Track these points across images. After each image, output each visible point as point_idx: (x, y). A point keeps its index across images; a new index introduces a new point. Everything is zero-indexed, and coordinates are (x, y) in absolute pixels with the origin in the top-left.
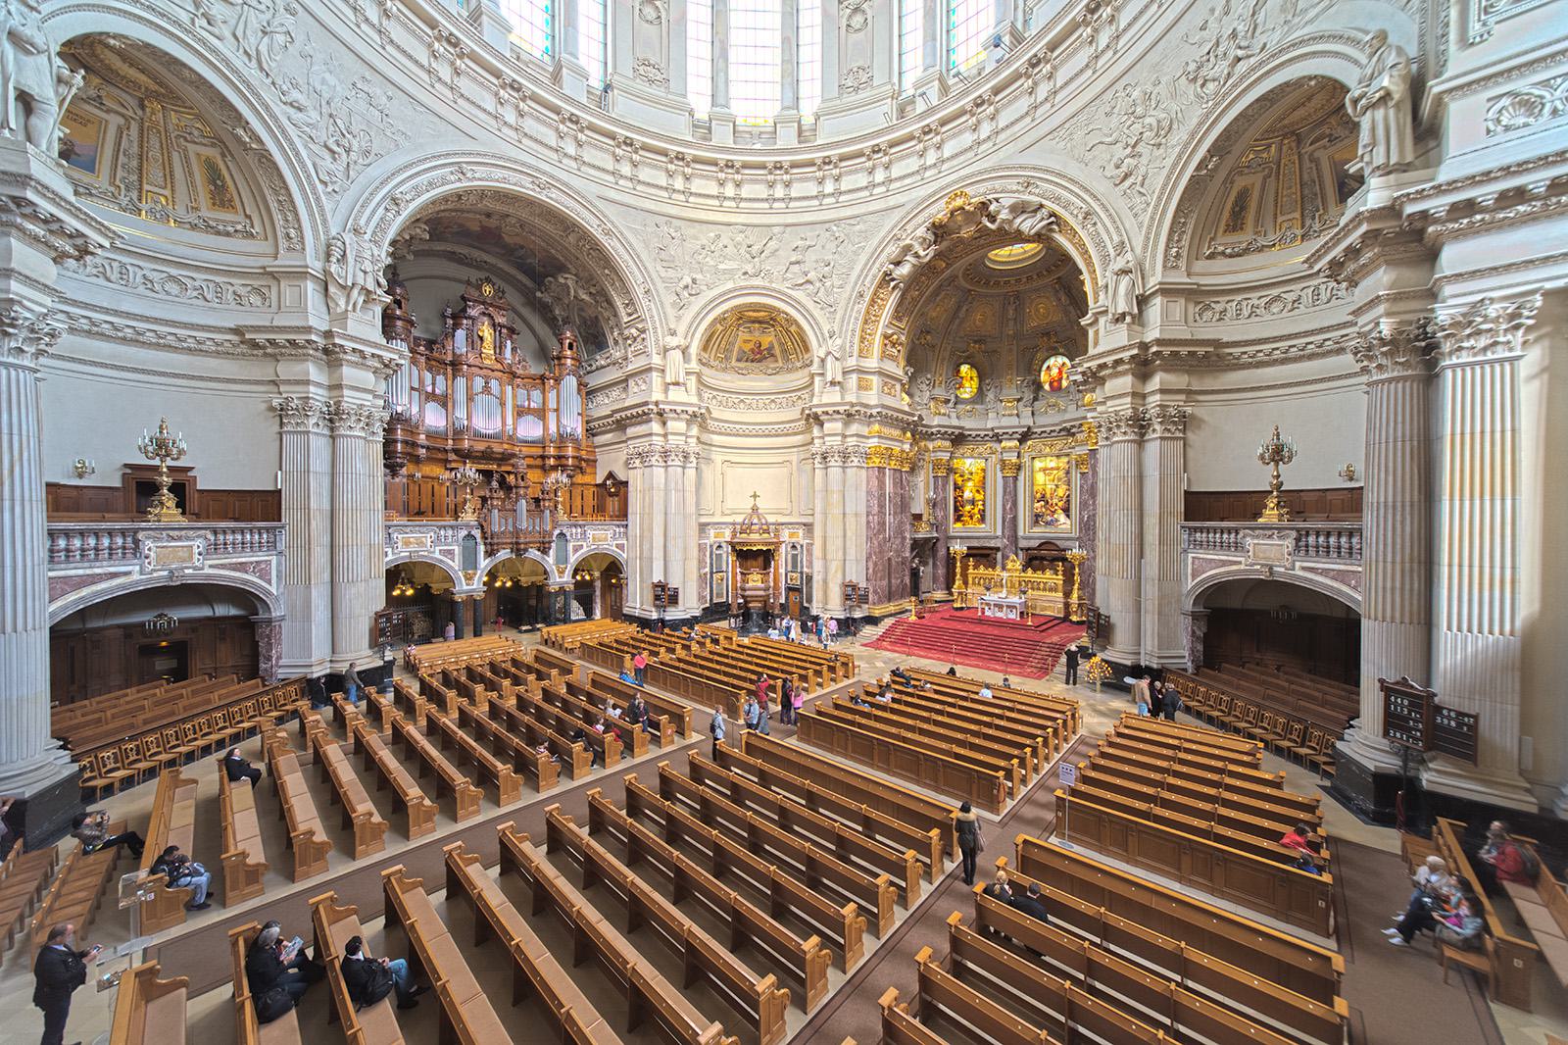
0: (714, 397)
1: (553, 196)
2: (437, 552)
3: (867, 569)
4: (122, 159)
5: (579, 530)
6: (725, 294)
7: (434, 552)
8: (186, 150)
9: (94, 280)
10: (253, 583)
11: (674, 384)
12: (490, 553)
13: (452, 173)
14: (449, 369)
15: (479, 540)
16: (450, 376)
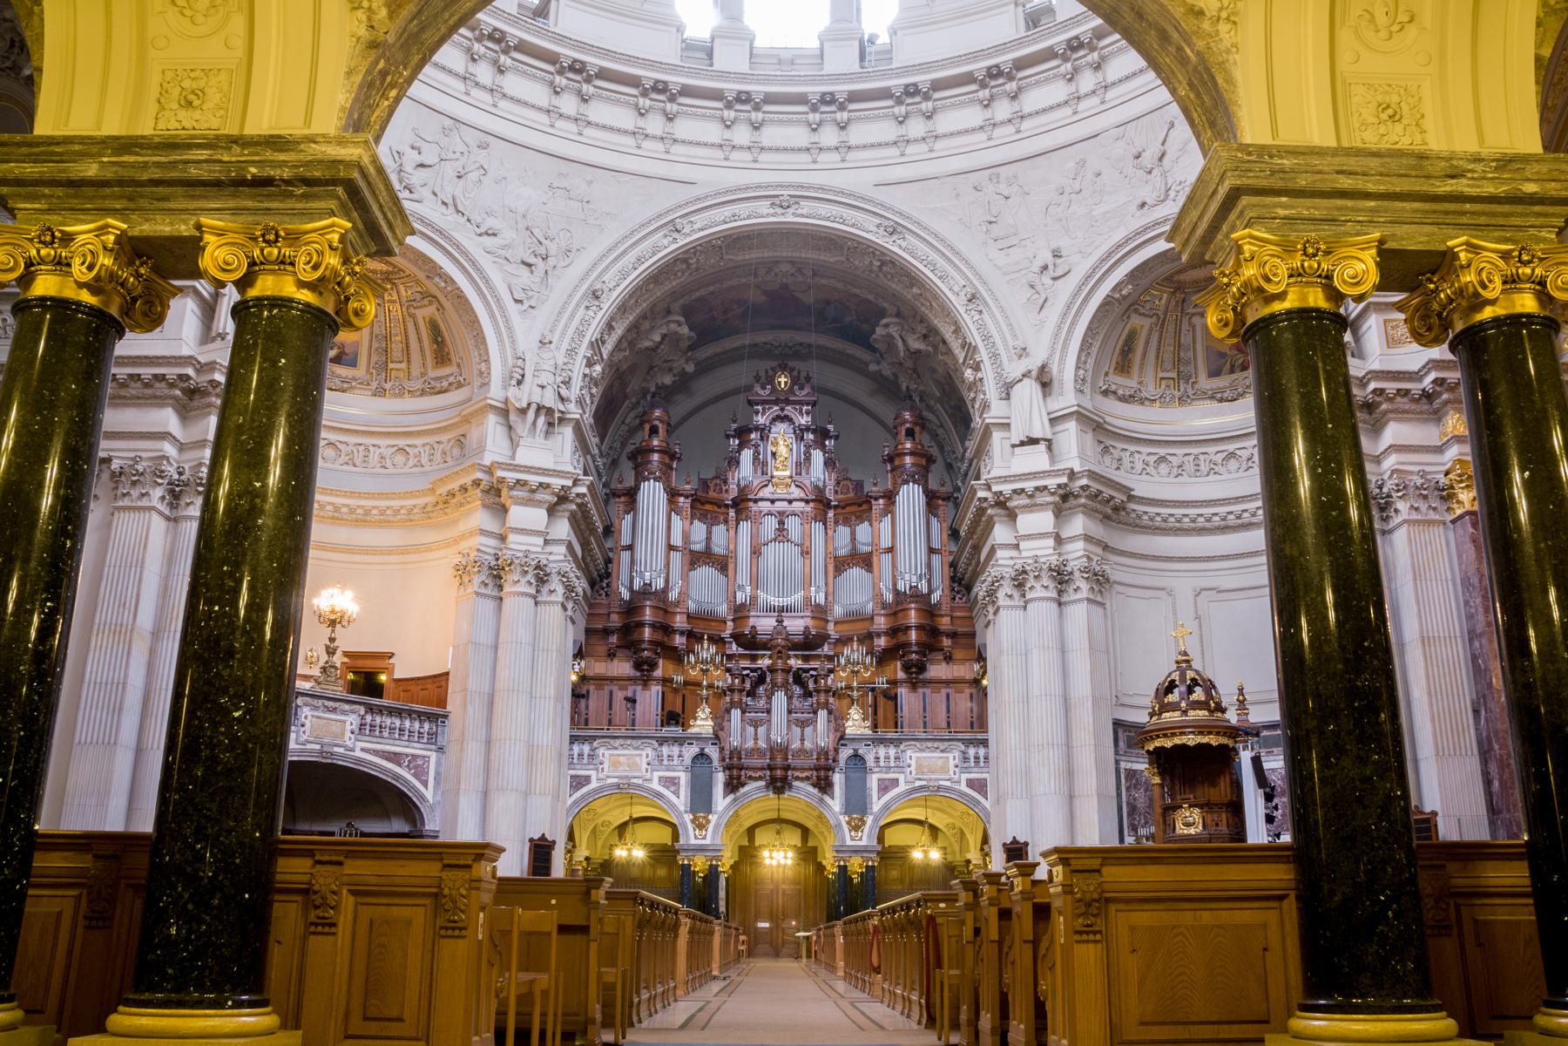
0: (1162, 459)
1: (804, 211)
2: (656, 780)
3: (1488, 783)
4: (375, 345)
5: (892, 751)
6: (1110, 254)
7: (650, 780)
8: (413, 316)
9: (345, 467)
10: (406, 781)
11: (1022, 444)
12: (732, 786)
13: (666, 236)
14: (732, 513)
15: (716, 763)
16: (732, 523)
